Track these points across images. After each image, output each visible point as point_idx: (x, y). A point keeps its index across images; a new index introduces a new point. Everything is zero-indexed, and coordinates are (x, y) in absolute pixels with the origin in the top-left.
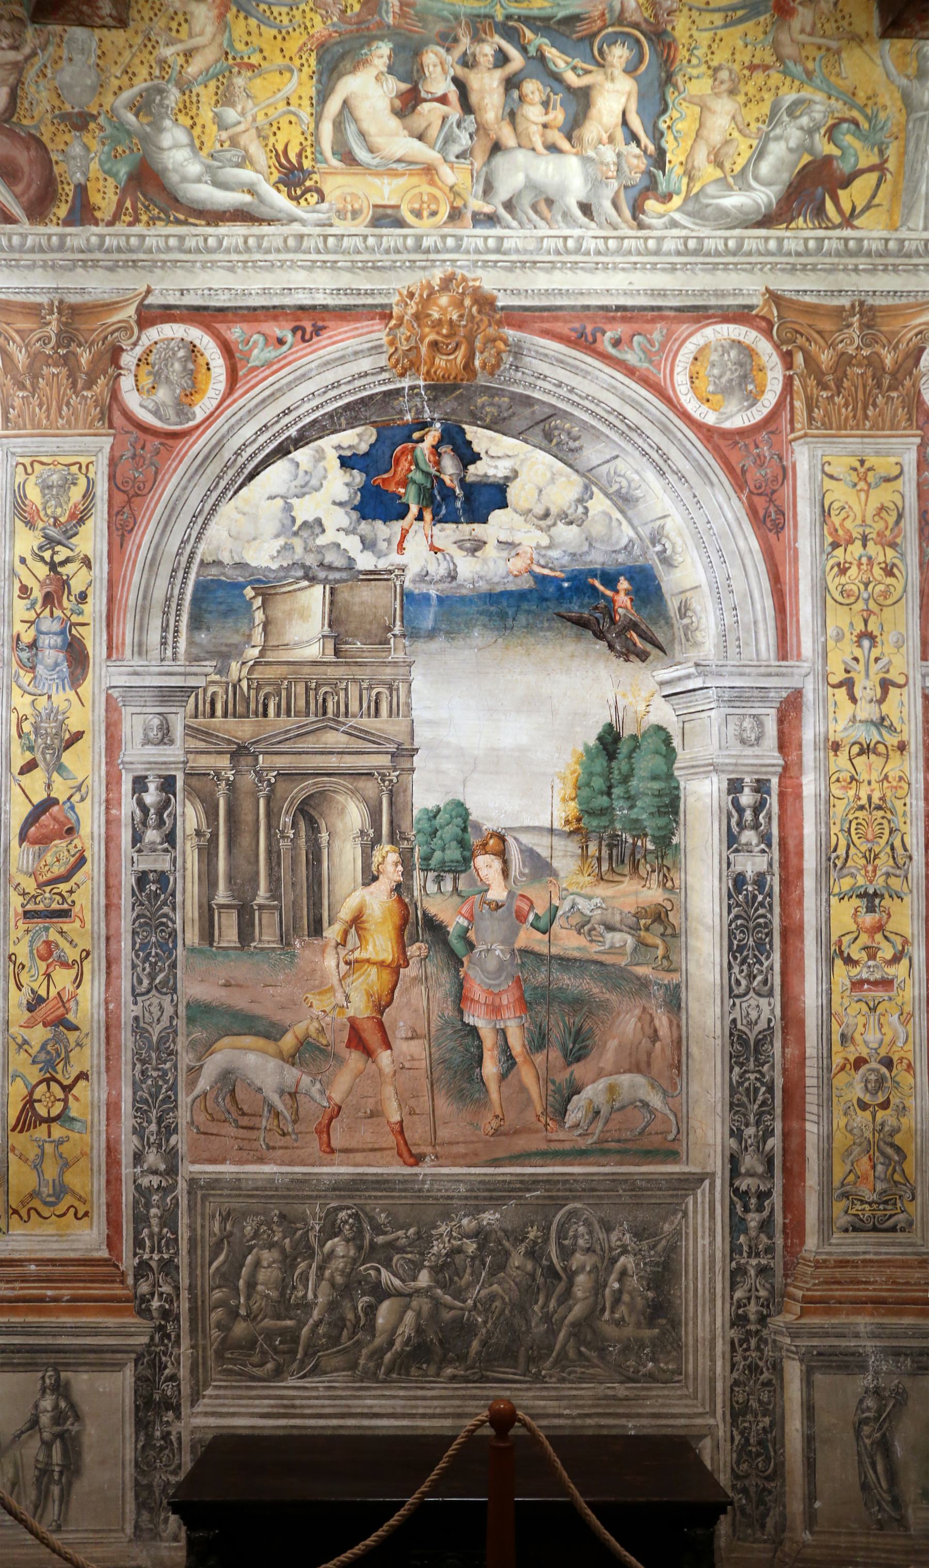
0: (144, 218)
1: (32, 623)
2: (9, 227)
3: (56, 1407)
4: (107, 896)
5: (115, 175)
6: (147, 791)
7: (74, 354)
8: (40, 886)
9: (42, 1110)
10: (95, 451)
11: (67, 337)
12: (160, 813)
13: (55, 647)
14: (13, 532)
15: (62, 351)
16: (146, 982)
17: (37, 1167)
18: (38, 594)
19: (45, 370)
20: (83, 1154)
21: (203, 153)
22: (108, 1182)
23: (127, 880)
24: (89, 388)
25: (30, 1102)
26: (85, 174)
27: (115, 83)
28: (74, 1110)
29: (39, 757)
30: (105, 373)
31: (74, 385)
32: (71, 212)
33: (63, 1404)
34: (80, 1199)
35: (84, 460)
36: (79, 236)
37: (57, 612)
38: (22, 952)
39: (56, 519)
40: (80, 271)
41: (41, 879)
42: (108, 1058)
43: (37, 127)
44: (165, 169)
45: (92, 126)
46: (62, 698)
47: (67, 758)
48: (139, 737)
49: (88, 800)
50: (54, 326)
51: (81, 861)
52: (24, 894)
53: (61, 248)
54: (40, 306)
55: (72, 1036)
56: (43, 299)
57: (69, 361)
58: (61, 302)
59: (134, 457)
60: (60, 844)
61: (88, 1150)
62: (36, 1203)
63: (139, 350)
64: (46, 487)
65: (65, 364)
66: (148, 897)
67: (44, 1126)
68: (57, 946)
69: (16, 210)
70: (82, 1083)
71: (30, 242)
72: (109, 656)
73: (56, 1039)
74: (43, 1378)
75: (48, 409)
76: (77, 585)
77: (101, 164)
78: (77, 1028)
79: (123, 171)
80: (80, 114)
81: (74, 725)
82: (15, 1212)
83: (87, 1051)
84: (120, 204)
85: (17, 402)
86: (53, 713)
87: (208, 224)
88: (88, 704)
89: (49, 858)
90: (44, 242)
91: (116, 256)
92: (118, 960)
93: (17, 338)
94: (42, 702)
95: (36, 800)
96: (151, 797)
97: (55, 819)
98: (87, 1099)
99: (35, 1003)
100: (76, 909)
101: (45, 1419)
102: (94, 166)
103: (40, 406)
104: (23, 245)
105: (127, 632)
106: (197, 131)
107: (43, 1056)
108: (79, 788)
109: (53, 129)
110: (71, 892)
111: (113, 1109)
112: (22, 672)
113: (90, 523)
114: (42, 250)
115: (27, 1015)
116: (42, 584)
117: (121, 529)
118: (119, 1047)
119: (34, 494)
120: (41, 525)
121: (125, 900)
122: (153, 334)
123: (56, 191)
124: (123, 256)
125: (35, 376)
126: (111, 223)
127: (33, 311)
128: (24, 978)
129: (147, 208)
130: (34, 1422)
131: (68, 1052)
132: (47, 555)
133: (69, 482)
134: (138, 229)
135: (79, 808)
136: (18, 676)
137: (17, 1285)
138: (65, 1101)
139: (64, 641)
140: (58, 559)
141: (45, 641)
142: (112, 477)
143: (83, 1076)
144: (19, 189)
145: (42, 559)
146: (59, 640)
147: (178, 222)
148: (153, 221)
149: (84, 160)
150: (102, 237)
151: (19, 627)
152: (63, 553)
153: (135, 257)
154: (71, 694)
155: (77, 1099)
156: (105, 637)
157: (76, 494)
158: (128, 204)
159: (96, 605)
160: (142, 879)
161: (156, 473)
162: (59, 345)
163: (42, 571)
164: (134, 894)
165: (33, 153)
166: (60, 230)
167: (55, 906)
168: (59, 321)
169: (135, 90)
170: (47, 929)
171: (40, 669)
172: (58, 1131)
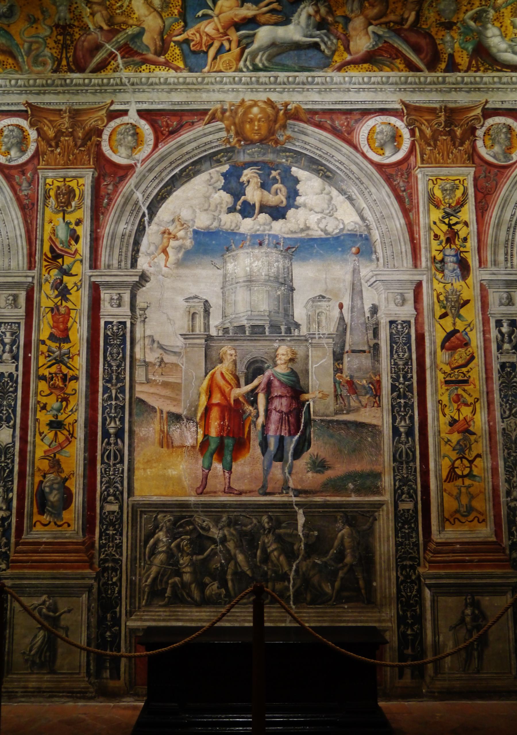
0: (482, 69)
1: (441, 251)
2: (419, 74)
3: (473, 613)
4: (486, 373)
5: (466, 49)
6: (502, 326)
7: (454, 130)
8: (453, 369)
9: (459, 472)
10: (467, 174)
11: (450, 122)
12: (510, 336)
13: (453, 262)
14: (429, 210)
15: (447, 129)
16: (508, 412)
17: (458, 498)
18: (443, 238)
19: (440, 138)
20: (481, 492)
21: (507, 39)
22: (494, 505)
23: (496, 366)
24: (462, 146)
25: (453, 468)
26: (453, 48)
27: (464, 8)
28: (475, 472)
29: (449, 311)
30: (469, 139)
31: (454, 145)
32: (447, 66)
33: (477, 612)
34: (480, 513)
35: (461, 178)
36: (452, 77)
37: (453, 246)
38: (445, 399)
39: (450, 205)
40: (454, 93)
41: (453, 366)
42: (491, 448)
43: (429, 29)
44: (490, 47)
45: (455, 28)
46: (458, 284)
47: (462, 311)
48: (497, 302)
49: (474, 331)
50: (442, 119)
51: (472, 358)
52: (444, 373)
53: (444, 82)
54: (435, 109)
55: (473, 438)
56: (437, 106)
57: (451, 133)
58: (445, 107)
59: (485, 177)
60: (461, 350)
61: (483, 490)
62: (458, 516)
63: (484, 129)
64: (444, 190)
65: (449, 135)
66: (506, 374)
67: (461, 480)
68: (462, 396)
69: (422, 66)
70: (478, 460)
71: (429, 80)
72: (480, 266)
73: (465, 439)
74: (466, 599)
75: (443, 155)
76: (462, 234)
77: (460, 44)
78: (474, 434)
79: (470, 47)
80: (449, 22)
81: (465, 296)
82: (448, 520)
83: (480, 444)
84: (470, 62)
85: (428, 152)
86: (454, 292)
87: (512, 71)
88: (472, 288)
89: (456, 356)
90: (435, 79)
91: (470, 86)
92: (493, 402)
93: (426, 123)
94: (449, 287)
95: (448, 330)
96: (505, 329)
97: (458, 339)
98: (482, 466)
99: (453, 422)
100: (471, 379)
101: (468, 619)
102: (457, 45)
103: (439, 153)
104: (426, 81)
105: (489, 255)
106: (503, 29)
107: (458, 447)
108: (469, 325)
109: (436, 29)
110: (468, 372)
111: (495, 470)
112: (437, 273)
113: (466, 207)
114: (434, 83)
115: (449, 428)
116: (445, 234)
117: (481, 210)
118: (496, 442)
119: (438, 193)
120: (442, 207)
121: (495, 375)
122: (490, 121)
123: (439, 57)
124: (473, 86)
125: (436, 140)
126: (466, 71)
127: (432, 111)
128: (446, 411)
129: (483, 64)
130: (462, 621)
131: (470, 445)
132: (446, 221)
133: (455, 188)
134: (479, 74)
135: (471, 334)
136: (435, 275)
137: (451, 555)
138: (471, 467)
139: (457, 259)
140: (452, 222)
141: (448, 259)
142: (475, 186)
143: (479, 456)
144: (422, 56)
145: (444, 223)
146: (455, 259)
147: (498, 71)
148: (486, 70)
149: (452, 43)
150: (463, 77)
151: (434, 253)
152: (454, 220)
153: (479, 86)
154: (462, 283)
155: (476, 466)
156: (477, 257)
157: (459, 193)
158: (474, 62)
159: (472, 243)
160: (503, 366)
161: (497, 184)
162: (446, 126)
163: (445, 228)
164: (499, 373)
165: (428, 40)
166: (442, 74)
167: (460, 378)
168: (445, 115)
169: (474, 11)
170: (457, 389)
171: (446, 271)
172: (467, 482)
